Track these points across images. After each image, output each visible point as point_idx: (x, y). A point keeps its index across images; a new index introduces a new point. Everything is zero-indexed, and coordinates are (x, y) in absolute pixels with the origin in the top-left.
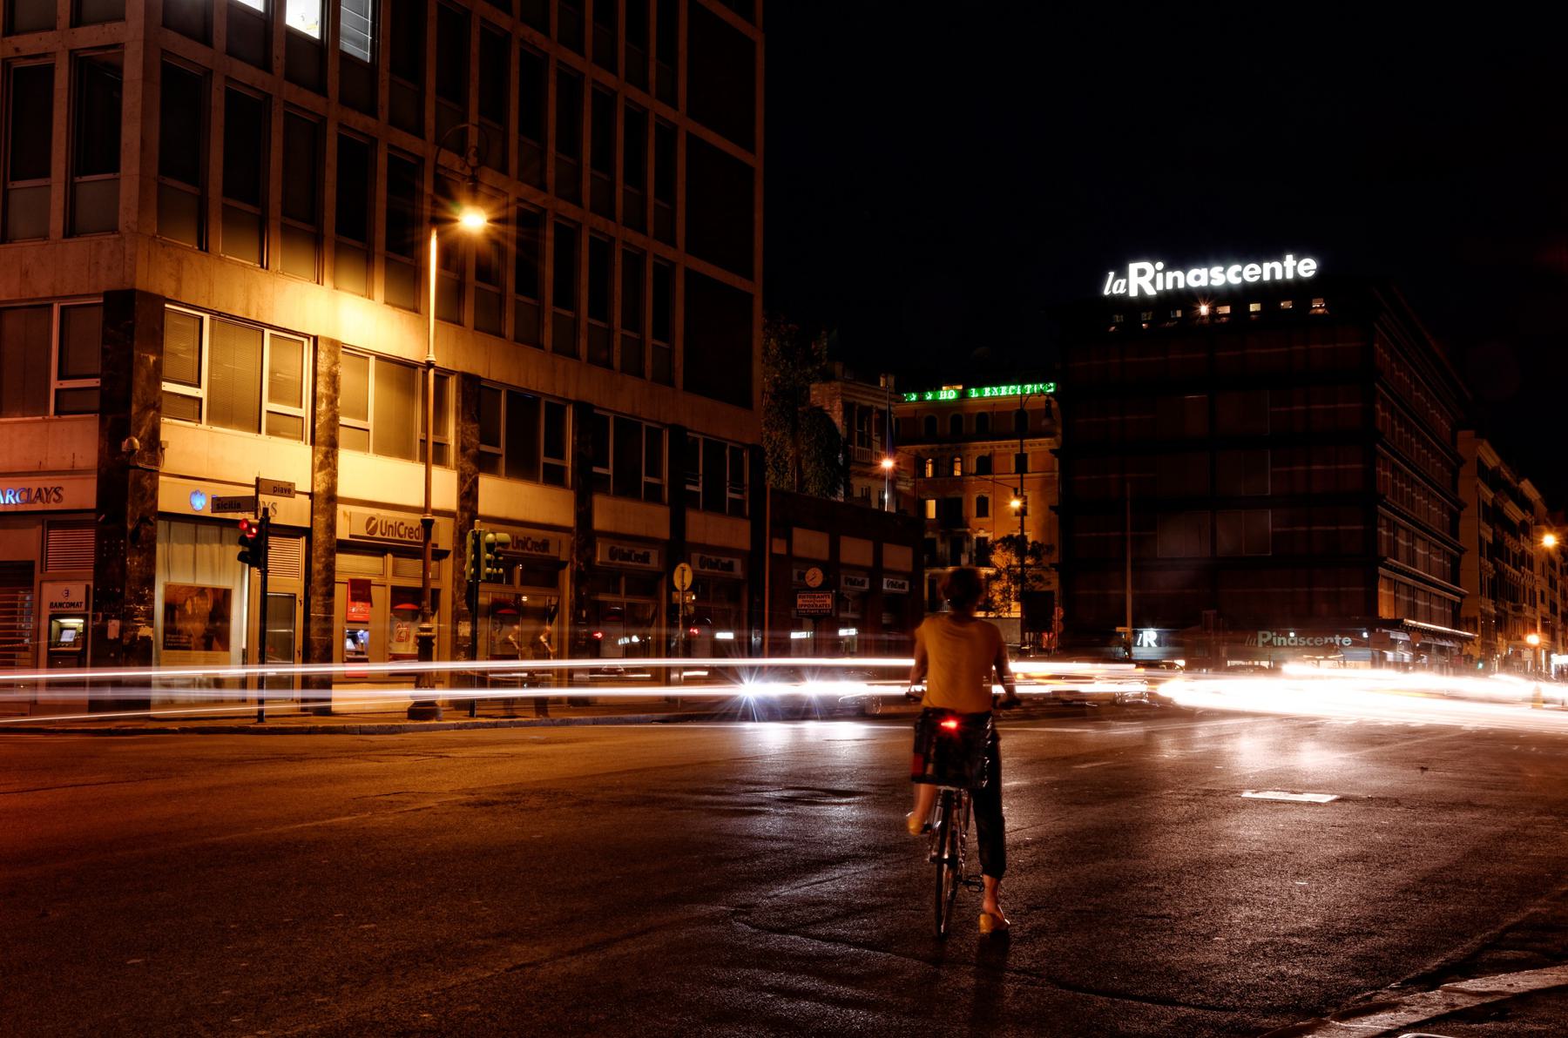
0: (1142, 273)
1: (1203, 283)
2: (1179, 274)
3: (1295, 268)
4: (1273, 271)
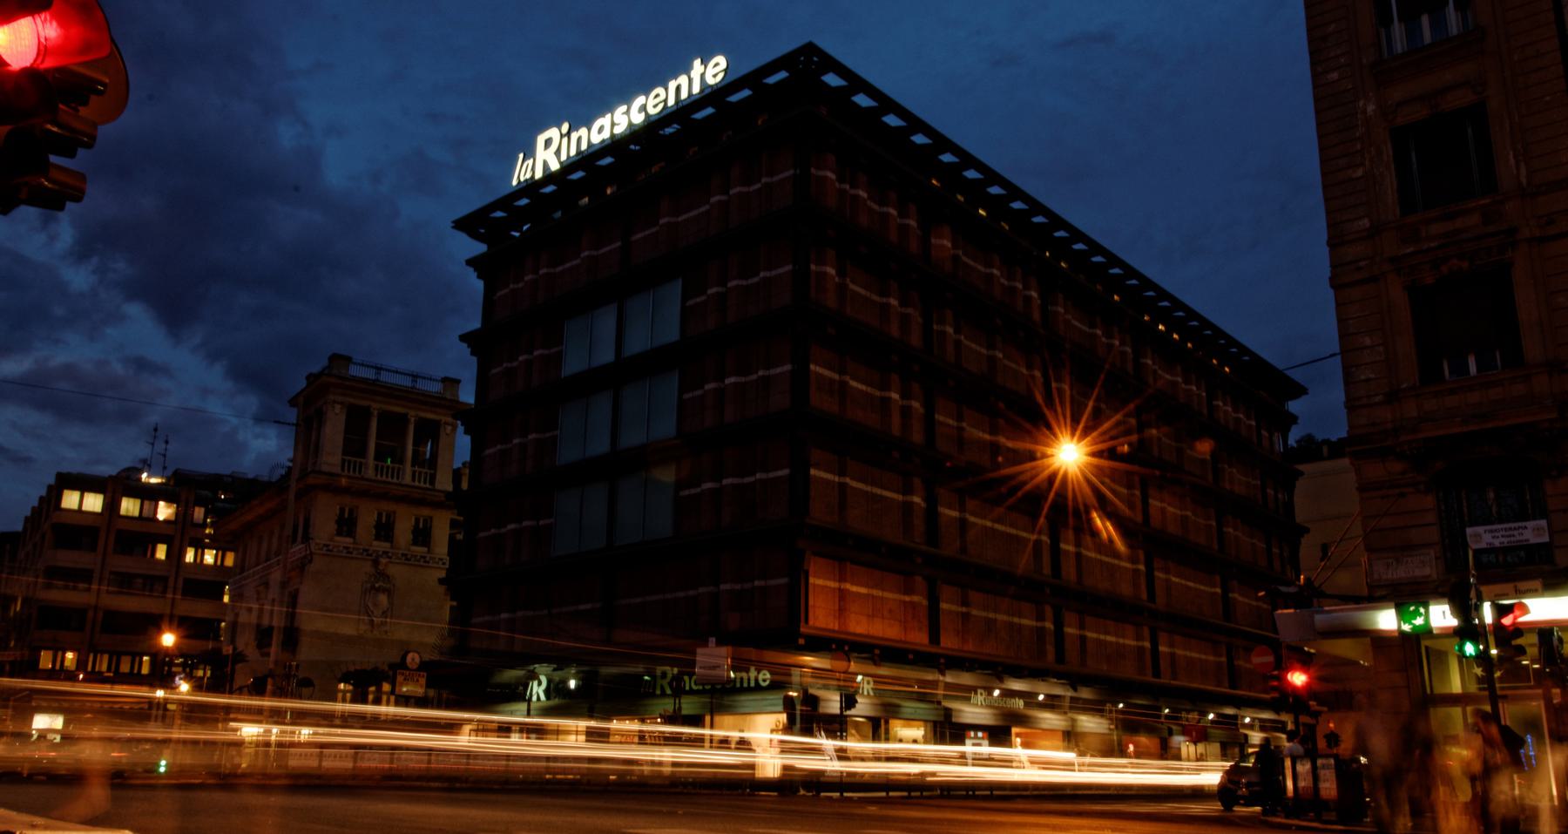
0: (548, 143)
1: (606, 135)
2: (583, 131)
3: (703, 76)
4: (678, 89)
